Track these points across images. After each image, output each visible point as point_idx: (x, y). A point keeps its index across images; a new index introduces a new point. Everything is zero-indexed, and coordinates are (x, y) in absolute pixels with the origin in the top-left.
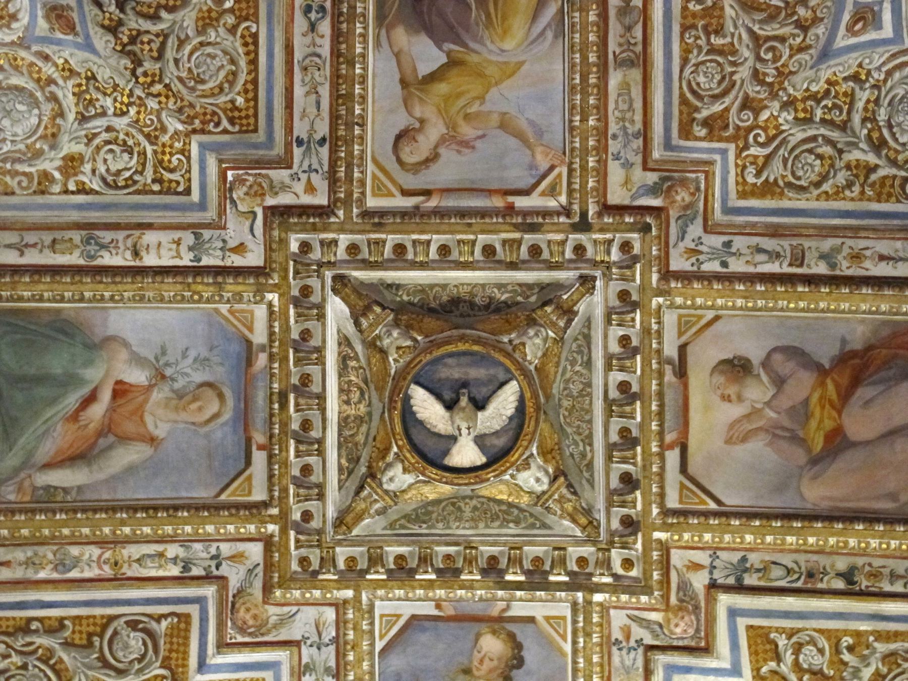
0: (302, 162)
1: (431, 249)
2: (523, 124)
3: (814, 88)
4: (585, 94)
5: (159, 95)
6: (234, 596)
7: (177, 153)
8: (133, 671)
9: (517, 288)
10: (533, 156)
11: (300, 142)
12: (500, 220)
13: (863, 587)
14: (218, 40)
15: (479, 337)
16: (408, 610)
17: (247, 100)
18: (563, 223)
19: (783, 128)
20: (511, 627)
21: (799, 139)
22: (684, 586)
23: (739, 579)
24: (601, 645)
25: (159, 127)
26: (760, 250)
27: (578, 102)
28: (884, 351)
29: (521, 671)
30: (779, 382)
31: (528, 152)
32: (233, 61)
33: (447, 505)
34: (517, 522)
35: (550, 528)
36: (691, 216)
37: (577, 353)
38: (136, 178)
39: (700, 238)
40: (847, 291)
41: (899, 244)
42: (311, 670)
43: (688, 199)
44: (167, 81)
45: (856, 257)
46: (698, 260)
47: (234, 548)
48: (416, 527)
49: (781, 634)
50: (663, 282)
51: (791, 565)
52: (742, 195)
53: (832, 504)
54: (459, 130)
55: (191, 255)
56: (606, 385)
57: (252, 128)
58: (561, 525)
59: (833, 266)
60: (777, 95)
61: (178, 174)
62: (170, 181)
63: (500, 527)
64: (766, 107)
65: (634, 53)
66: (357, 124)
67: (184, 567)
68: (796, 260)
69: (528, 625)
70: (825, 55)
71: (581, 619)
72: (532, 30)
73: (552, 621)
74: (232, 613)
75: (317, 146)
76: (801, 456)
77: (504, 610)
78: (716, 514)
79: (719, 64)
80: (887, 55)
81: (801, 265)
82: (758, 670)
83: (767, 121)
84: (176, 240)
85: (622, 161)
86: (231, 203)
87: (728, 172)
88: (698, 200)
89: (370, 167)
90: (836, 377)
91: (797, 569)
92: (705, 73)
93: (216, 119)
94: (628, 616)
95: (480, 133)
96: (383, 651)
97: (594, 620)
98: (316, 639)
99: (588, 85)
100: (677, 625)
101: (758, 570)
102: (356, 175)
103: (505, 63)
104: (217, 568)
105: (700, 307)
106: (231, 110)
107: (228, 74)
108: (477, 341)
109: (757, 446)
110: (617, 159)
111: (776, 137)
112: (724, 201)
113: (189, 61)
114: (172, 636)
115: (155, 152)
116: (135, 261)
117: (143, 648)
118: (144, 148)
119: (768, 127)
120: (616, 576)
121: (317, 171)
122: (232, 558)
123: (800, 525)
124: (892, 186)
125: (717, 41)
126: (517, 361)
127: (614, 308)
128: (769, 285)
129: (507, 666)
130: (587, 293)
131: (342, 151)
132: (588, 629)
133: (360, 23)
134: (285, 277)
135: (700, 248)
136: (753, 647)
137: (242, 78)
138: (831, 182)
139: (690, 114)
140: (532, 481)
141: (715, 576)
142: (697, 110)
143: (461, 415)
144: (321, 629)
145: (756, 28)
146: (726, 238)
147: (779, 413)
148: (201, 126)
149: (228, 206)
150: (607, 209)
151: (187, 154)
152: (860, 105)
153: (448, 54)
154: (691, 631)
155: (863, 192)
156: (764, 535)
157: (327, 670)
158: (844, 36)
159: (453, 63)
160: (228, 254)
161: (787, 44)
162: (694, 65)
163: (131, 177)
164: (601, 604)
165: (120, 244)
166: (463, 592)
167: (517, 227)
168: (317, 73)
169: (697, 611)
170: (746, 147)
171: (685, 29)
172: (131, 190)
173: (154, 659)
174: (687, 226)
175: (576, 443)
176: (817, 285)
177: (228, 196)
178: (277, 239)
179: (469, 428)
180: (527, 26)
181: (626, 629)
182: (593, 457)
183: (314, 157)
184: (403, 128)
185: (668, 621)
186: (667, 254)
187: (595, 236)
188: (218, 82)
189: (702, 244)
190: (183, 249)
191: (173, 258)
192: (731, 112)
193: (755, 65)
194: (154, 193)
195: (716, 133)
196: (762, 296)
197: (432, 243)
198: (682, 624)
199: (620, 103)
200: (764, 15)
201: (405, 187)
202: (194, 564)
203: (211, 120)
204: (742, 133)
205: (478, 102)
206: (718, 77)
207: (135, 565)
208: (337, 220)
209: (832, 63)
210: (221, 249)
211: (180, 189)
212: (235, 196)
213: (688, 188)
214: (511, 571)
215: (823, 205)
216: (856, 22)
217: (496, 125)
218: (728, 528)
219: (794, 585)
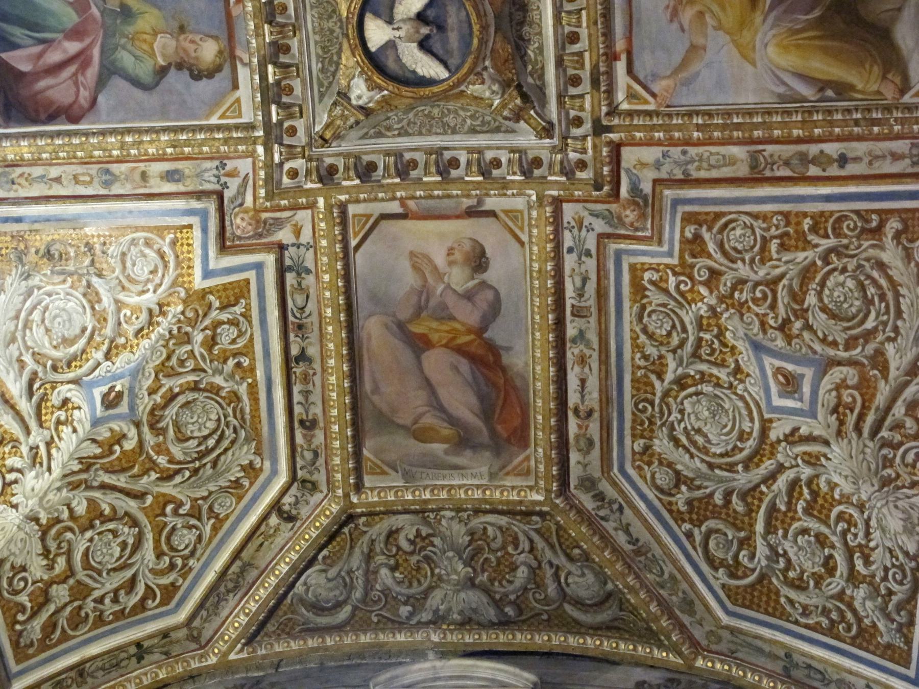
2: (695, 67)
3: (728, 335)
4: (724, 127)
9: (540, 65)
10: (664, 78)
12: (601, 51)
13: (294, 370)
15: (486, 43)
18: (600, 110)
20: (227, 69)
22: (279, 224)
23: (290, 269)
26: (585, 280)
27: (715, 121)
28: (502, 381)
30: (469, 296)
31: (669, 73)
33: (332, 5)
34: (323, 70)
35: (320, 101)
37: (483, 121)
39: (593, 230)
40: (551, 355)
41: (596, 395)
43: (627, 220)
45: (582, 360)
46: (573, 227)
50: (550, 200)
52: (633, 268)
53: (365, 341)
56: (455, 149)
58: (324, 111)
59: (574, 341)
60: (722, 302)
63: (318, 56)
65: (764, 169)
68: (578, 311)
69: (231, 83)
70: (757, 347)
72: (787, 74)
76: (404, 314)
78: (345, 249)
79: (752, 248)
80: (757, 398)
81: (573, 314)
82: (211, 293)
85: (661, 159)
88: (627, 229)
90: (476, 343)
91: (304, 315)
92: (744, 235)
95: (686, 27)
97: (239, 147)
99: (731, 131)
100: (243, 219)
101: (299, 284)
103: (754, 47)
105: (530, 231)
108: (483, 42)
109: (410, 279)
110: (664, 156)
111: (686, 299)
120: (281, 164)
123: (342, 319)
124: (646, 392)
125: (774, 246)
126: (467, 78)
127: (526, 153)
128: (553, 291)
129: (192, 65)
130: (537, 132)
132: (231, 142)
135: (584, 230)
138: (647, 342)
139: (705, 222)
140: (358, 92)
142: (710, 229)
143: (412, 31)
146: (594, 252)
147: (441, 295)
150: (616, 148)
152: (715, 371)
154: (238, 233)
155: (639, 368)
156: (330, 291)
158: (774, 366)
161: (768, 311)
162: (752, 225)
164: (255, 151)
166: (253, 27)
167: (595, 68)
171: (786, 215)
174: (603, 219)
175: (400, 121)
176: (555, 330)
179: (399, 37)
180: (790, 69)
182: (389, 137)
185: (246, 211)
189: (588, 231)
193: (751, 281)
196: (543, 285)
198: (244, 224)
199: (717, 157)
204: (688, 271)
205: (715, 24)
206: (740, 247)
209: (750, 352)
213: (637, 221)
214: (276, 70)
215: (627, 335)
216: (784, 376)
217: (694, 42)
218: (333, 257)
219: (290, 314)
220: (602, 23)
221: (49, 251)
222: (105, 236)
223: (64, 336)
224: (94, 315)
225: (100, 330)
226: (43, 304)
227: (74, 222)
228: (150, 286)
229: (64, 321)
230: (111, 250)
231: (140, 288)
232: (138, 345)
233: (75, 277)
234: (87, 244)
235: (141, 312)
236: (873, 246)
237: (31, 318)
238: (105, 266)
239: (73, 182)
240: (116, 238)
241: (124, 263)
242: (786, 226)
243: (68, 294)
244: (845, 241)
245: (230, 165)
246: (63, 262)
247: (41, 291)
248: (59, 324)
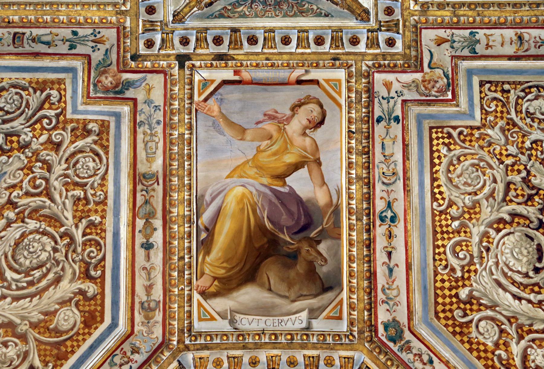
0: (395, 105)
1: (296, 42)
4: (181, 155)
5: (507, 156)
7: (492, 112)
11: (397, 119)
14: (463, 197)
17: (438, 151)
19: (29, 129)
21: (17, 121)
25: (506, 132)
26: (48, 44)
27: (186, 148)
32: (450, 180)
36: (100, 66)
38: (522, 94)
43: (103, 78)
44: (501, 166)
46: (95, 36)
52: (60, 82)
54: (276, 127)
55: (477, 37)
57: (434, 130)
61: (489, 97)
62: (495, 91)
64: (42, 144)
66: (353, 133)
75: (384, 117)
79: (78, 176)
83: (41, 134)
84: (490, 48)
85: (153, 105)
86: (448, 75)
87: (72, 97)
88: (95, 78)
89: (343, 101)
93: (462, 137)
102: (353, 95)
106: (450, 143)
107: (454, 170)
110: (156, 106)
112: (75, 78)
113: (485, 181)
115: (508, 113)
116: (521, 33)
118: (517, 116)
119: (40, 130)
121: (383, 98)
125: (79, 192)
130: (179, 13)
131: (364, 113)
133: (352, 208)
134: (405, 22)
135: (94, 44)
137: (442, 168)
139: (101, 139)
142: (95, 142)
145: (48, 202)
146: (73, 51)
148: (473, 132)
149: (450, 73)
151: (484, 111)
153: (285, 183)
159: (281, 177)
160: (449, 38)
162: (97, 175)
163: (527, 94)
165: (533, 44)
168: (385, 171)
170: (58, 116)
171: (104, 203)
172: (526, 85)
174: (103, 59)
177: (450, 80)
178: (412, 49)
183: (386, 109)
184: (319, 130)
186: (118, 40)
187: (174, 52)
188: (462, 164)
189: (92, 47)
190: (484, 41)
191: (492, 35)
192: (69, 140)
194: (509, 83)
195: (81, 126)
197: (295, 46)
200: (42, 212)
201: (316, 86)
203: (465, 136)
206: (79, 166)
208: (367, 62)
210: (455, 41)
211: (488, 86)
212: (445, 80)
220: (267, 64)
236: (74, 273)
242: (94, 201)
244: (79, 249)
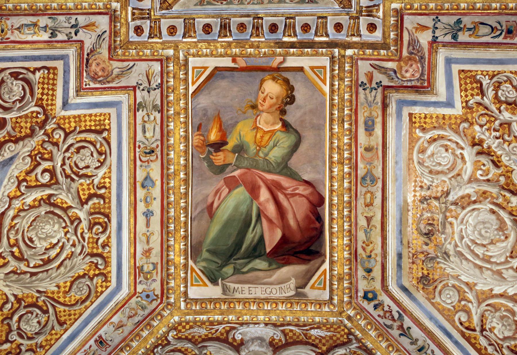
6: (88, 55)
8: (16, 109)
16: (212, 63)
22: (413, 43)
24: (351, 87)
29: (292, 106)
42: (143, 107)
47: (87, 19)
48: (219, 4)
49: (485, 76)
51: (494, 25)
67: (52, 34)
69: (298, 73)
71: (337, 68)
73: (315, 70)
74: (87, 67)
77: (281, 63)
91: (499, 28)
94: (371, 65)
96: (194, 92)
97: (346, 69)
98: (146, 84)
100: (407, 71)
101: (469, 29)
104: (76, 35)
114: (43, 83)
117: (23, 92)
122: (86, 27)
136: (464, 85)
141: (436, 35)
144: (150, 78)
154: (417, 75)
157: (155, 107)
164: (351, 57)
166: (252, 50)
169: (422, 60)
173: (31, 100)
181: (369, 75)
185: (401, 68)
198: (411, 70)
202: (59, 32)
207: (16, 32)
221: (426, 234)
222: (415, 186)
223: (497, 229)
224: (480, 202)
225: (492, 197)
226: (470, 244)
227: (403, 210)
228: (458, 152)
229: (485, 228)
230: (426, 182)
231: (459, 161)
232: (506, 166)
233: (448, 214)
234: (421, 202)
235: (480, 161)
237: (481, 256)
238: (440, 189)
239: (371, 207)
240: (417, 177)
241: (438, 173)
243: (462, 222)
245: (363, 78)
246: (435, 223)
247: (459, 244)
248: (486, 232)
